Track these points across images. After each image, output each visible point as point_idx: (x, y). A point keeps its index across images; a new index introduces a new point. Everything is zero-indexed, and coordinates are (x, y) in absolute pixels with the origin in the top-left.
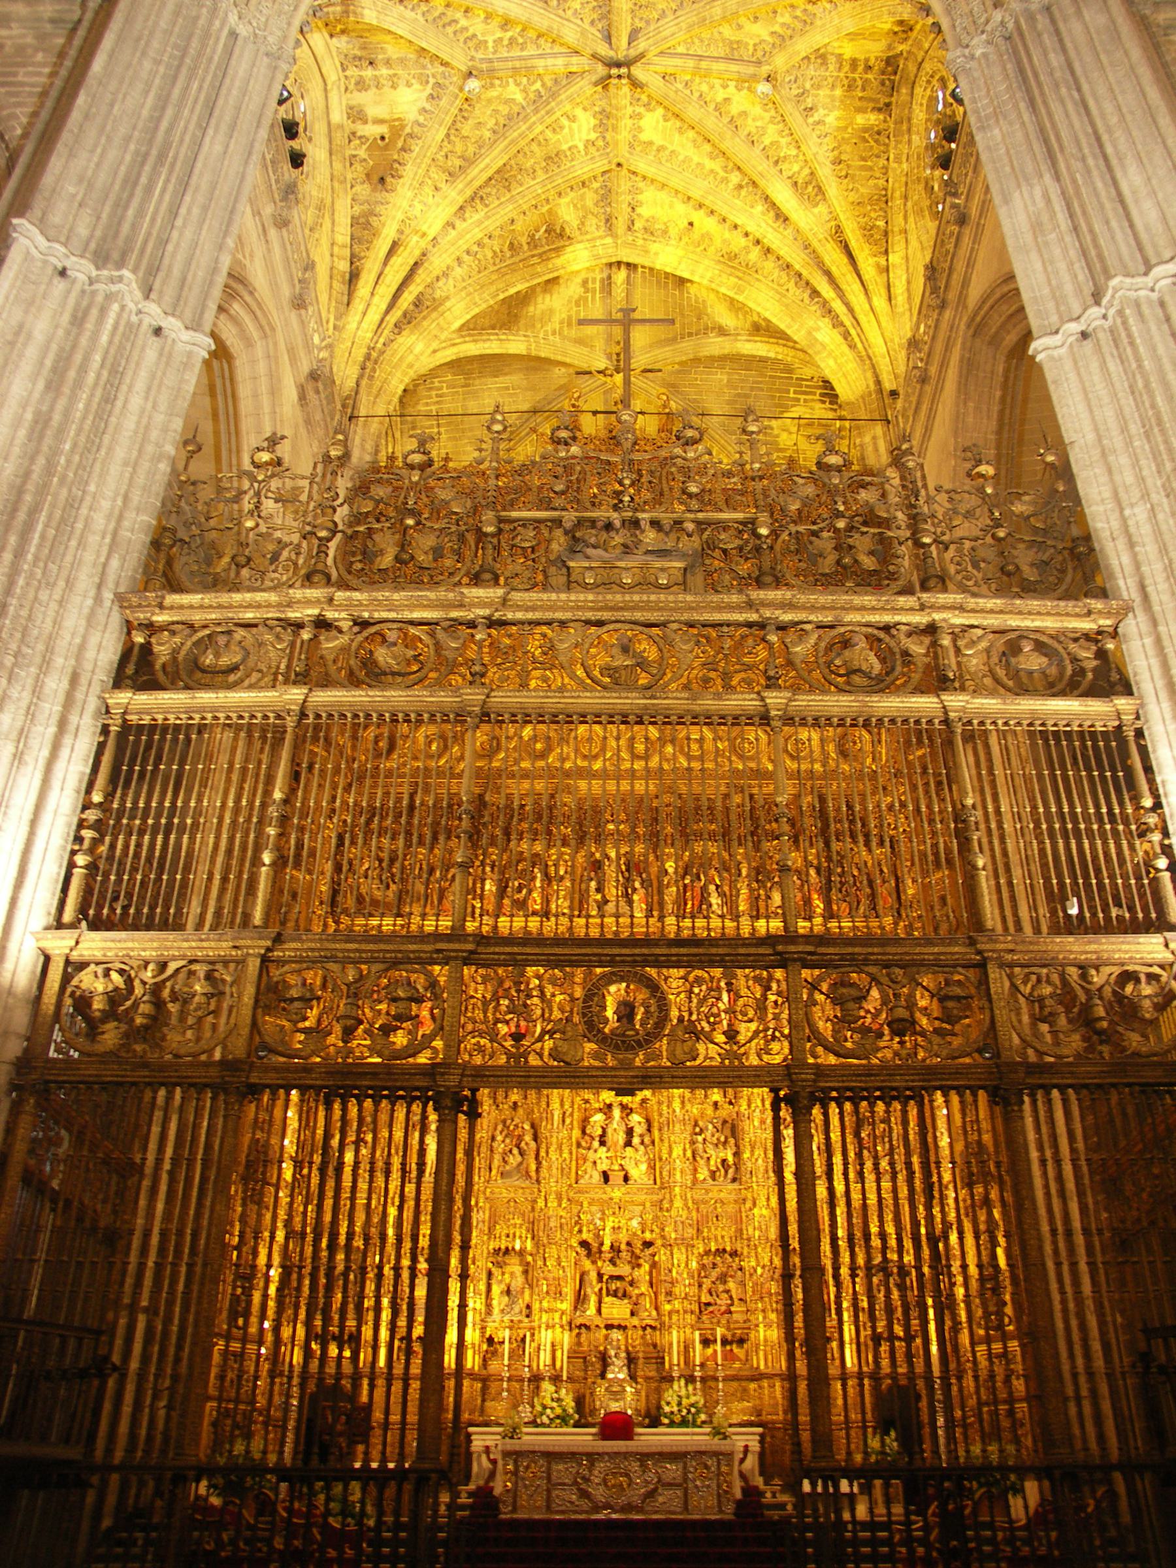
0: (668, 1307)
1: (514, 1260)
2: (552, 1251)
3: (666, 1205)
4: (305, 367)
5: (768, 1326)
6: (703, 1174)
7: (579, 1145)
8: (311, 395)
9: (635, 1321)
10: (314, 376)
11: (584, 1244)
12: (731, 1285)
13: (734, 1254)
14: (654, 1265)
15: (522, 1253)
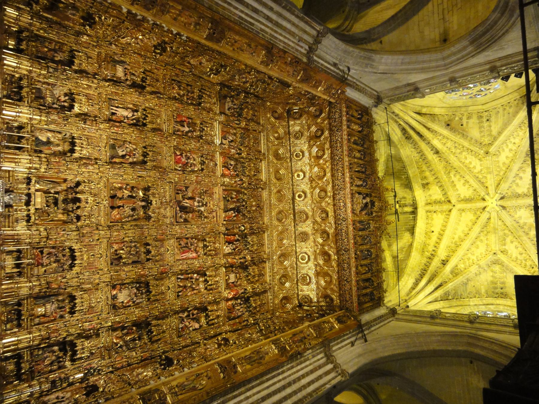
0: (42, 229)
1: (67, 147)
2: (75, 166)
3: (100, 228)
4: (420, 86)
5: (31, 288)
6: (116, 247)
7: (127, 185)
8: (408, 88)
9: (32, 211)
10: (417, 89)
11: (78, 184)
12: (55, 265)
13: (72, 266)
14: (65, 222)
15: (72, 151)
